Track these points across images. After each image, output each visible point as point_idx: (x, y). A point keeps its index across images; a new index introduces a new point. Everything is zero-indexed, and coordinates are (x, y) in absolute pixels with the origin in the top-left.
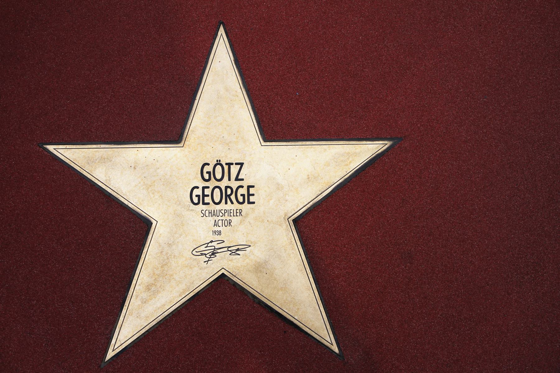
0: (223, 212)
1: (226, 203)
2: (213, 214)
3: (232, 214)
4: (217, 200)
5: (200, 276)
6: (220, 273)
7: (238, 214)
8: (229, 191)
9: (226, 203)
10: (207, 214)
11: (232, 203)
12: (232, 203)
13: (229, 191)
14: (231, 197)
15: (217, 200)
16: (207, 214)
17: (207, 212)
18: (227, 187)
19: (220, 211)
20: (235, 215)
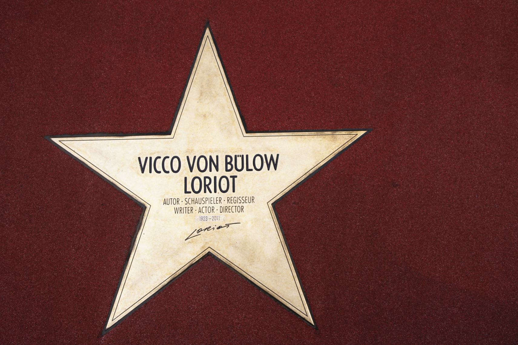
0: (204, 200)
1: (205, 192)
2: (195, 201)
3: (212, 202)
4: (197, 189)
5: (190, 254)
6: (207, 252)
7: (218, 202)
8: (208, 181)
9: (205, 192)
10: (190, 202)
11: (211, 192)
12: (211, 192)
13: (208, 181)
14: (210, 186)
15: (197, 188)
16: (190, 202)
17: (190, 200)
18: (205, 178)
19: (202, 199)
20: (215, 202)
